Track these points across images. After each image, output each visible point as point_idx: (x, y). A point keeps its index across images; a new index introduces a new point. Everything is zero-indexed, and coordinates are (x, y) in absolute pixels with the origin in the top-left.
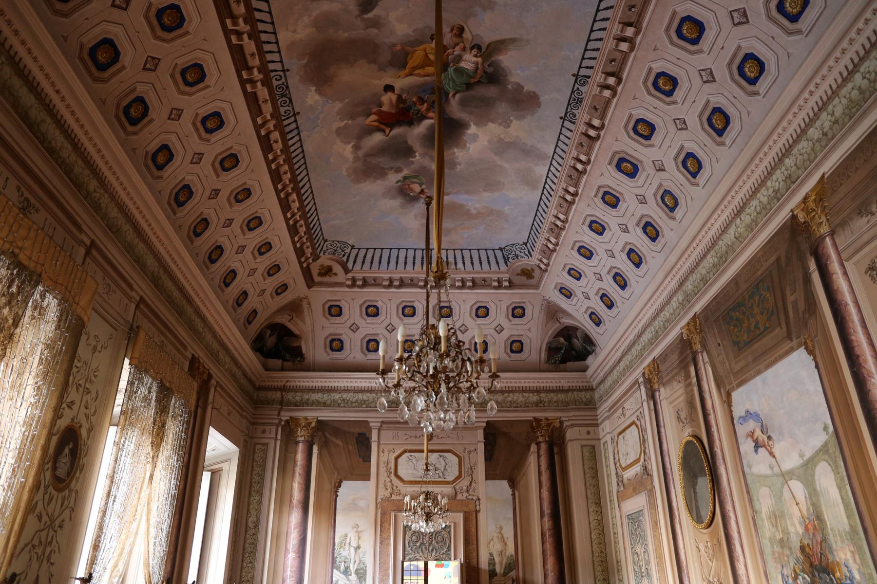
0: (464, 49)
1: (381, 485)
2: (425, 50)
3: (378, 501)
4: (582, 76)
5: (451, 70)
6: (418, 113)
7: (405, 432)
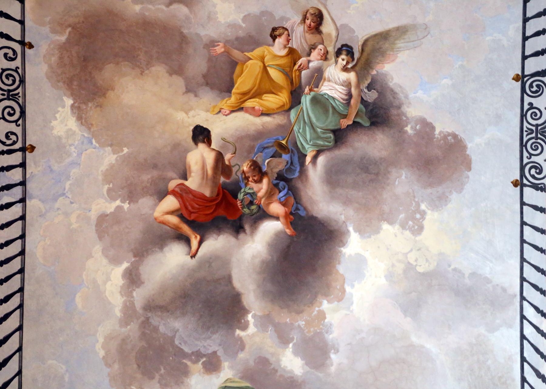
0: (325, 57)
2: (262, 59)
4: (533, 75)
5: (306, 100)
6: (251, 203)
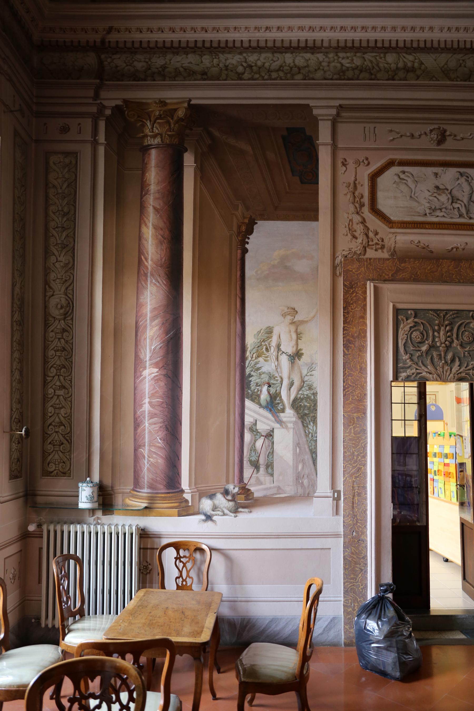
1: (342, 230)
3: (338, 261)
7: (389, 127)
